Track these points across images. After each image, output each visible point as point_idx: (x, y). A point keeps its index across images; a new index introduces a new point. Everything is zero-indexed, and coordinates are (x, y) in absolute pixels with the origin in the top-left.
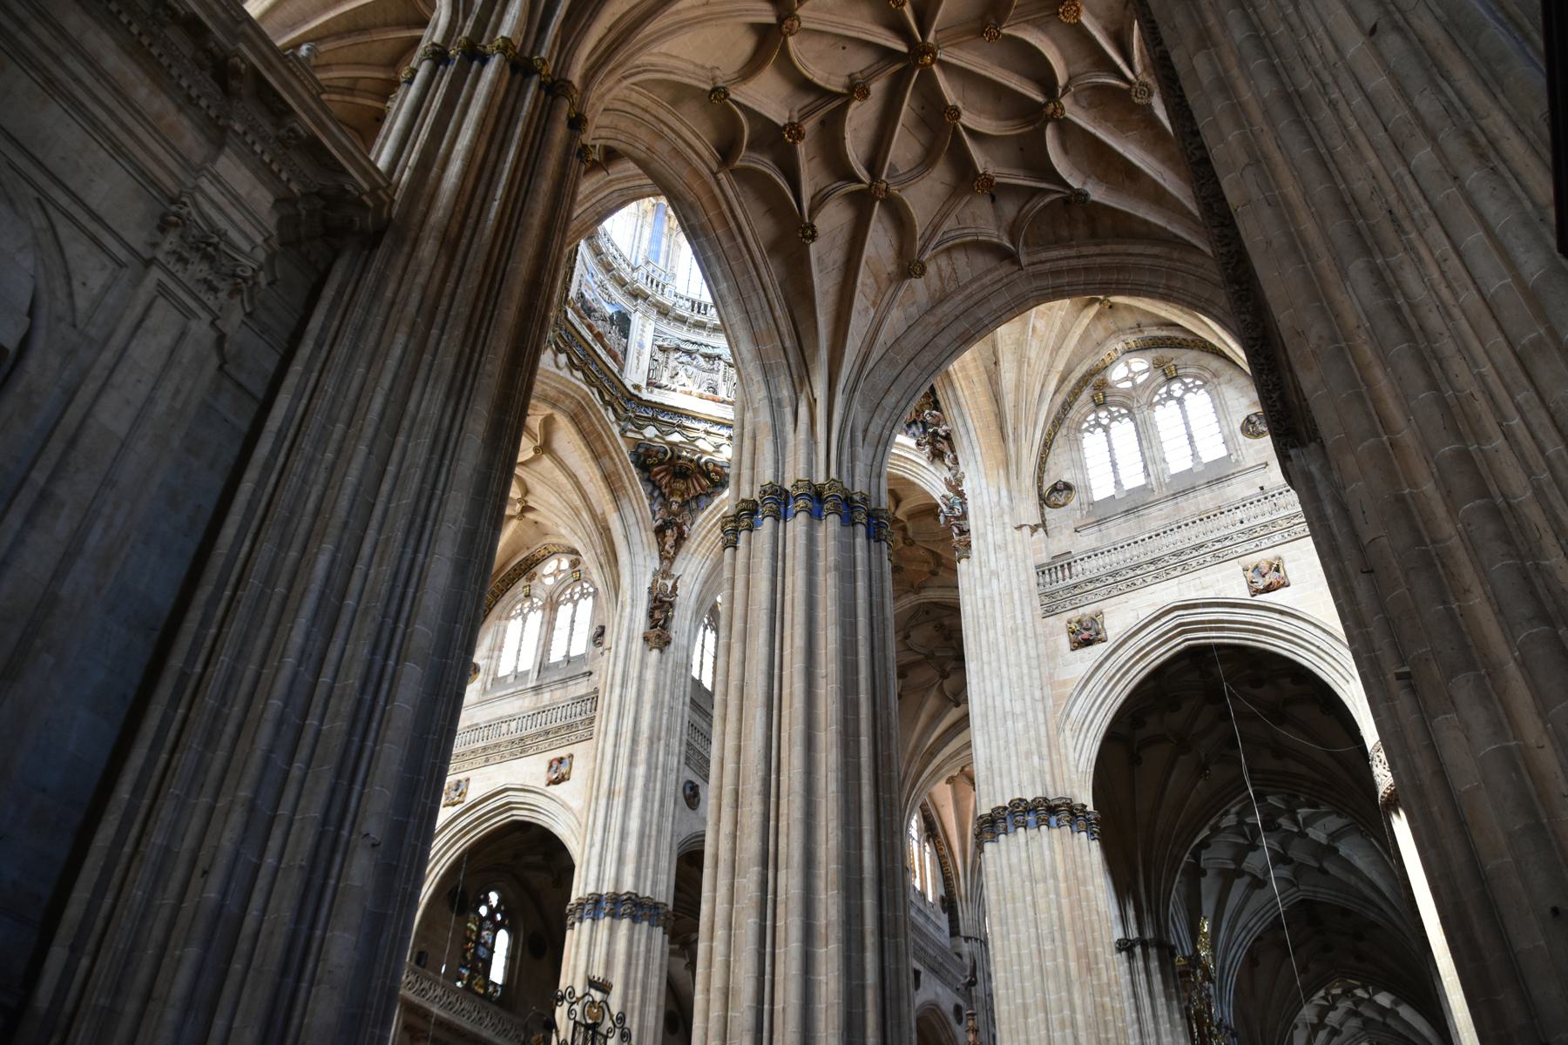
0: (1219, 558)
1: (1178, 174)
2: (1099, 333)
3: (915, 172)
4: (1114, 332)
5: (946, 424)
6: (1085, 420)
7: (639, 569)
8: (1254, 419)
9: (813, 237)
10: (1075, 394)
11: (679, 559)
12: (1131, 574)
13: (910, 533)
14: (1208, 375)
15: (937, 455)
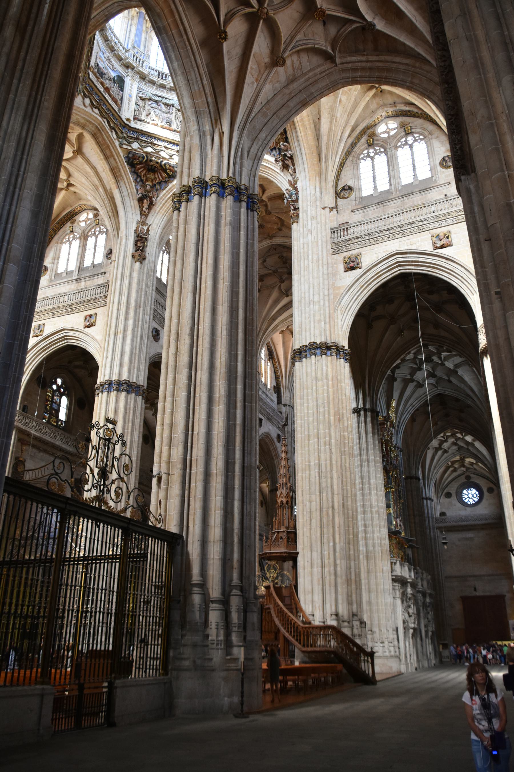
0: (421, 230)
1: (424, 18)
2: (374, 106)
3: (283, 4)
4: (381, 106)
5: (291, 150)
6: (362, 153)
7: (129, 220)
8: (447, 159)
9: (225, 39)
10: (358, 138)
11: (150, 215)
12: (377, 235)
13: (269, 208)
14: (426, 133)
15: (285, 167)
